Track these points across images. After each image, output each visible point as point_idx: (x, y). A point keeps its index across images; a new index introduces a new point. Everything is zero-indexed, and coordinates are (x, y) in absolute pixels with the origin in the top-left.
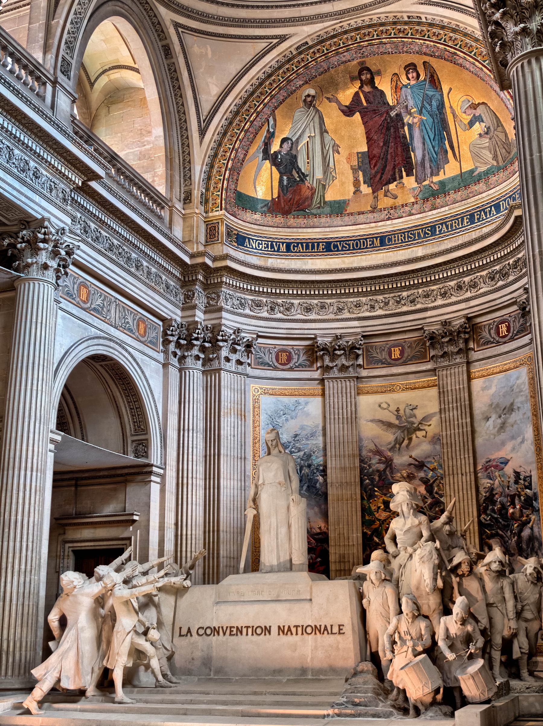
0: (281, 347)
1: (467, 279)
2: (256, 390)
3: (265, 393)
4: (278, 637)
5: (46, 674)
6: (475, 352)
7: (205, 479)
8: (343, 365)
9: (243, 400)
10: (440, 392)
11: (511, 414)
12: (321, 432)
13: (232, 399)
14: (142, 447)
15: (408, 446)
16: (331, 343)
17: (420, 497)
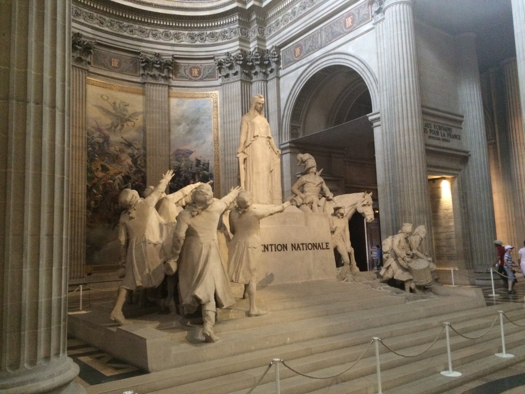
1: (172, 31)
6: (173, 80)
10: (147, 100)
15: (121, 130)
17: (127, 166)
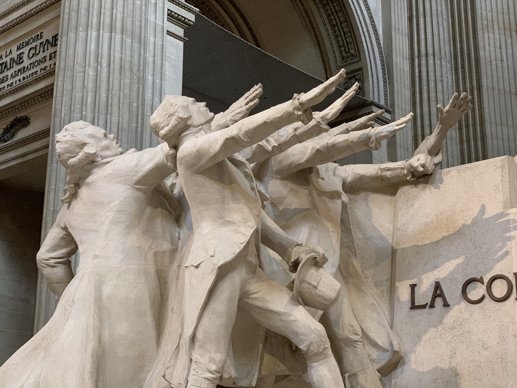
13: (494, 6)
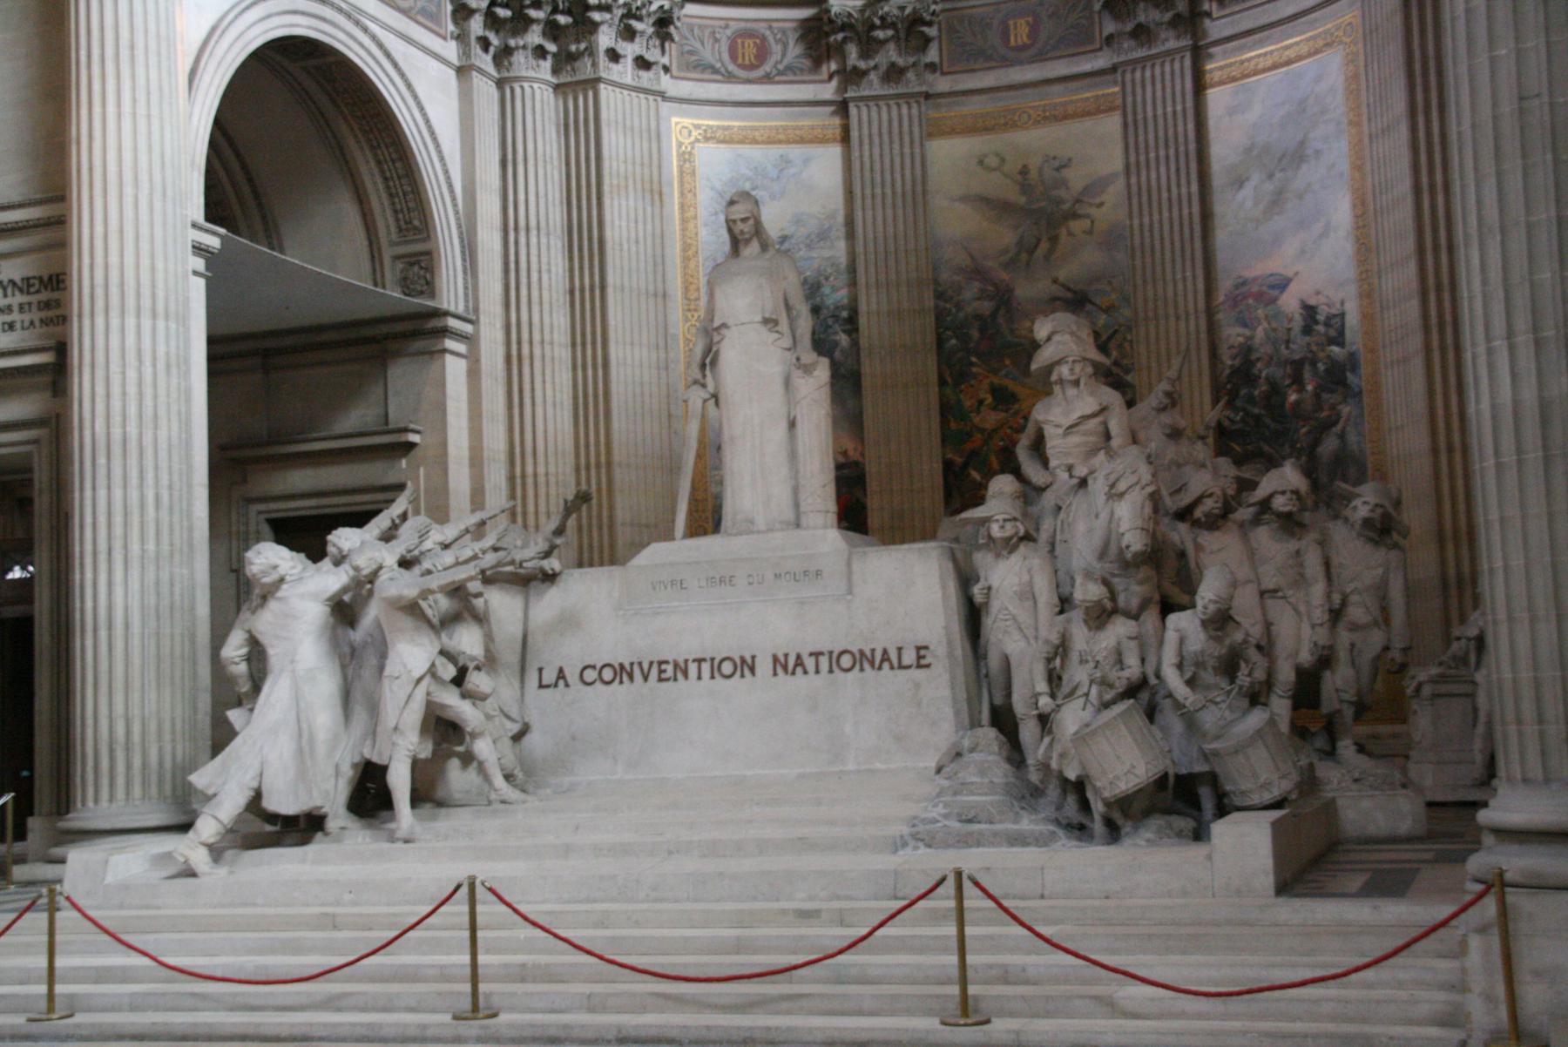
0: (743, 25)
2: (685, 132)
3: (707, 139)
4: (774, 680)
5: (226, 787)
6: (1214, 20)
7: (574, 345)
8: (893, 65)
9: (655, 156)
10: (1125, 125)
11: (1298, 167)
12: (843, 230)
13: (629, 153)
14: (420, 268)
15: (1047, 257)
16: (862, 11)
